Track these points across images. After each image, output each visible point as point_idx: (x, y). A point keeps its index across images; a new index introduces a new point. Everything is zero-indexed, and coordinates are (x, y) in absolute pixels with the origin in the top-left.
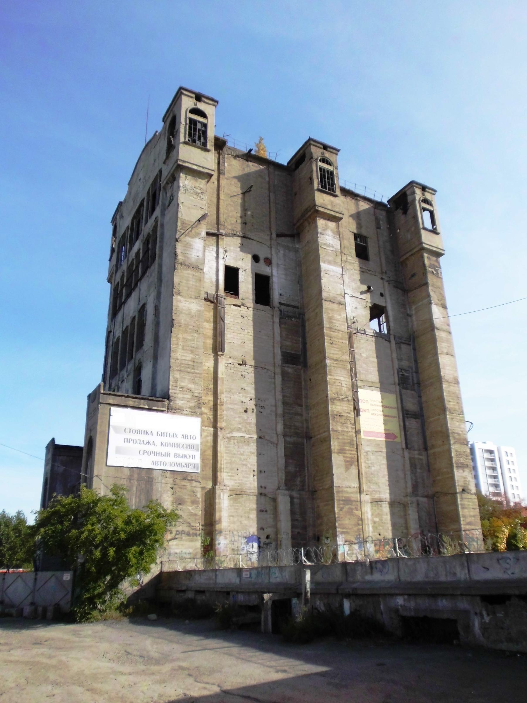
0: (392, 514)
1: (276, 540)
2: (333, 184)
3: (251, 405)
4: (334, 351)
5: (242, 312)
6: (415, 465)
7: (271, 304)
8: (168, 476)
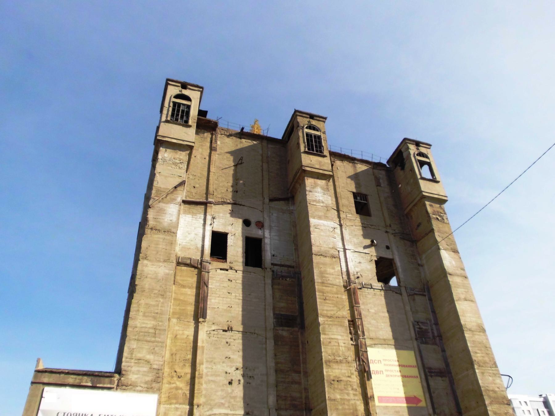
2: (321, 146)
3: (238, 375)
5: (229, 275)
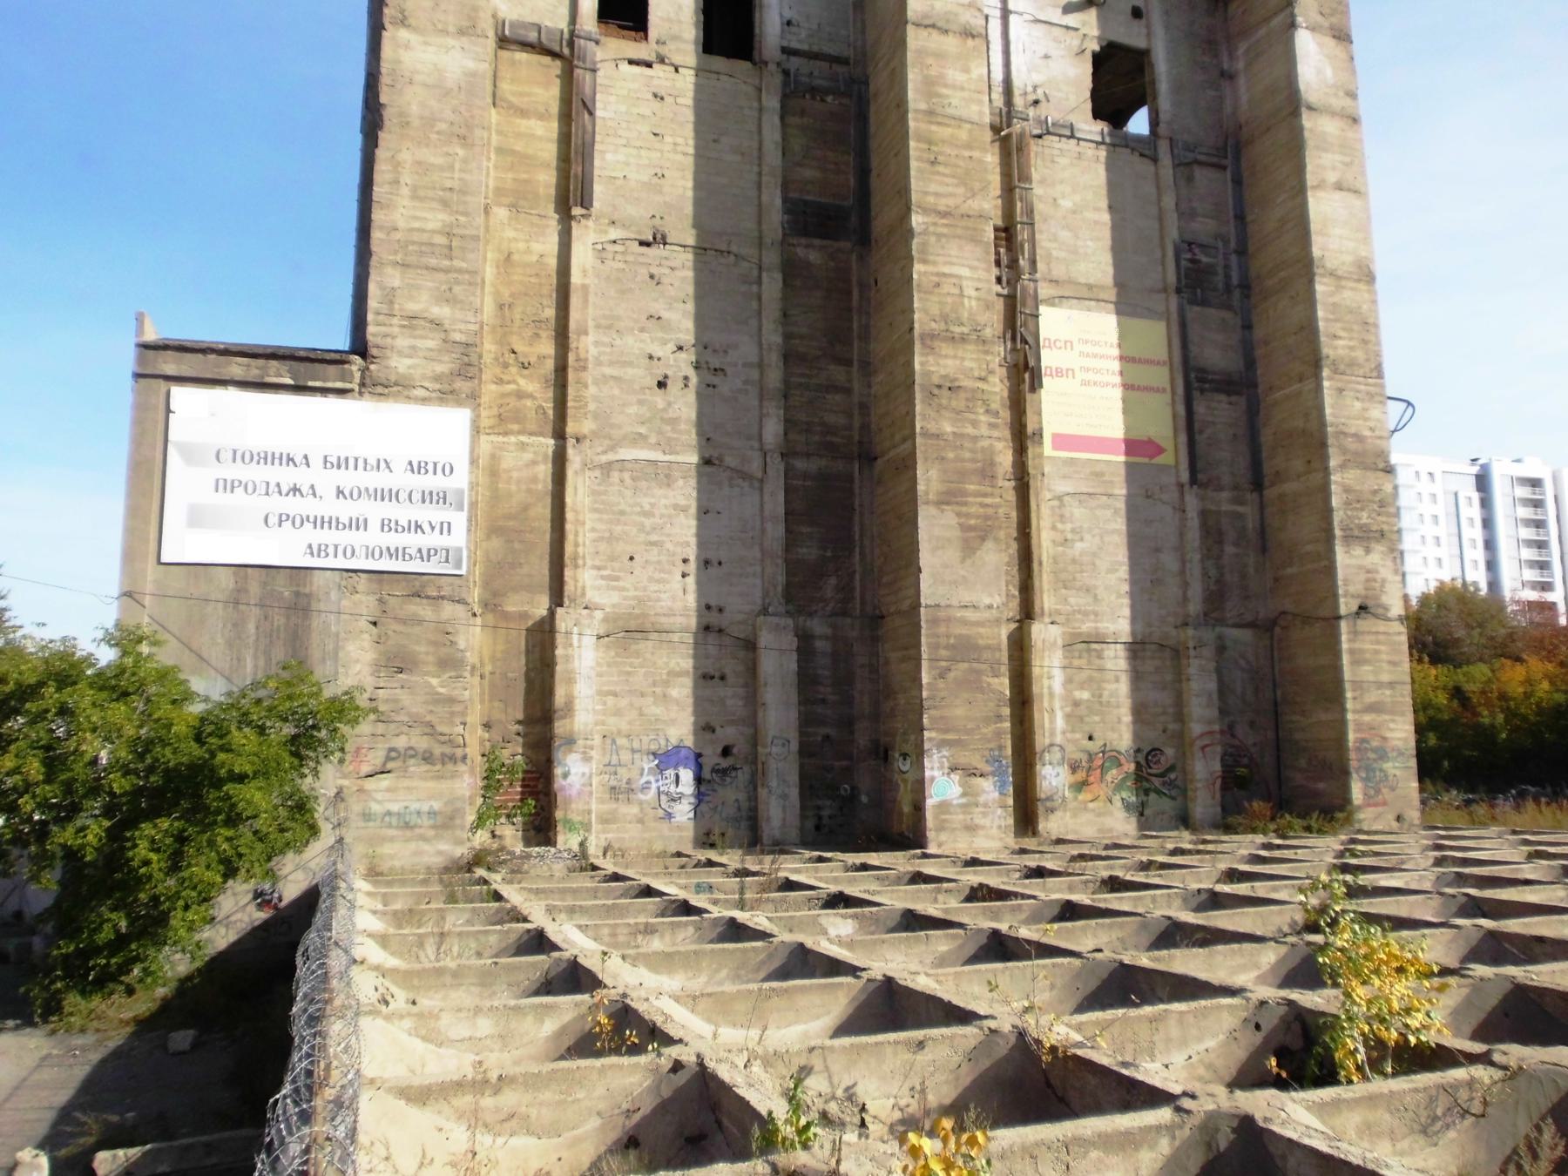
0: (1137, 677)
1: (753, 759)
3: (682, 366)
4: (944, 185)
5: (656, 82)
6: (1220, 533)
7: (756, 57)
8: (360, 588)
